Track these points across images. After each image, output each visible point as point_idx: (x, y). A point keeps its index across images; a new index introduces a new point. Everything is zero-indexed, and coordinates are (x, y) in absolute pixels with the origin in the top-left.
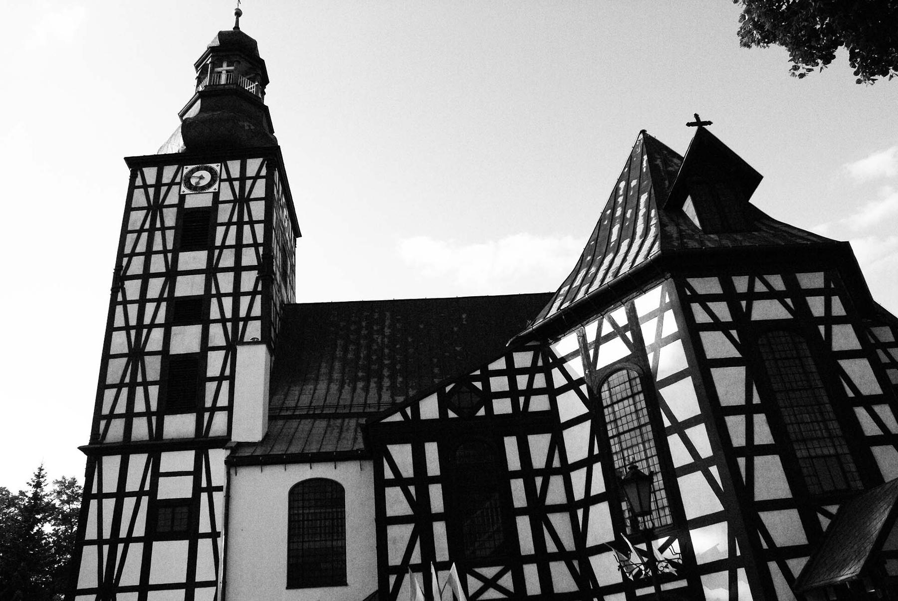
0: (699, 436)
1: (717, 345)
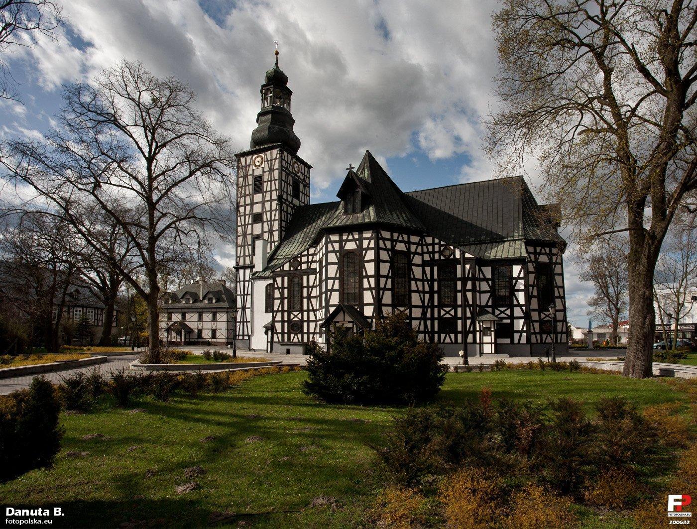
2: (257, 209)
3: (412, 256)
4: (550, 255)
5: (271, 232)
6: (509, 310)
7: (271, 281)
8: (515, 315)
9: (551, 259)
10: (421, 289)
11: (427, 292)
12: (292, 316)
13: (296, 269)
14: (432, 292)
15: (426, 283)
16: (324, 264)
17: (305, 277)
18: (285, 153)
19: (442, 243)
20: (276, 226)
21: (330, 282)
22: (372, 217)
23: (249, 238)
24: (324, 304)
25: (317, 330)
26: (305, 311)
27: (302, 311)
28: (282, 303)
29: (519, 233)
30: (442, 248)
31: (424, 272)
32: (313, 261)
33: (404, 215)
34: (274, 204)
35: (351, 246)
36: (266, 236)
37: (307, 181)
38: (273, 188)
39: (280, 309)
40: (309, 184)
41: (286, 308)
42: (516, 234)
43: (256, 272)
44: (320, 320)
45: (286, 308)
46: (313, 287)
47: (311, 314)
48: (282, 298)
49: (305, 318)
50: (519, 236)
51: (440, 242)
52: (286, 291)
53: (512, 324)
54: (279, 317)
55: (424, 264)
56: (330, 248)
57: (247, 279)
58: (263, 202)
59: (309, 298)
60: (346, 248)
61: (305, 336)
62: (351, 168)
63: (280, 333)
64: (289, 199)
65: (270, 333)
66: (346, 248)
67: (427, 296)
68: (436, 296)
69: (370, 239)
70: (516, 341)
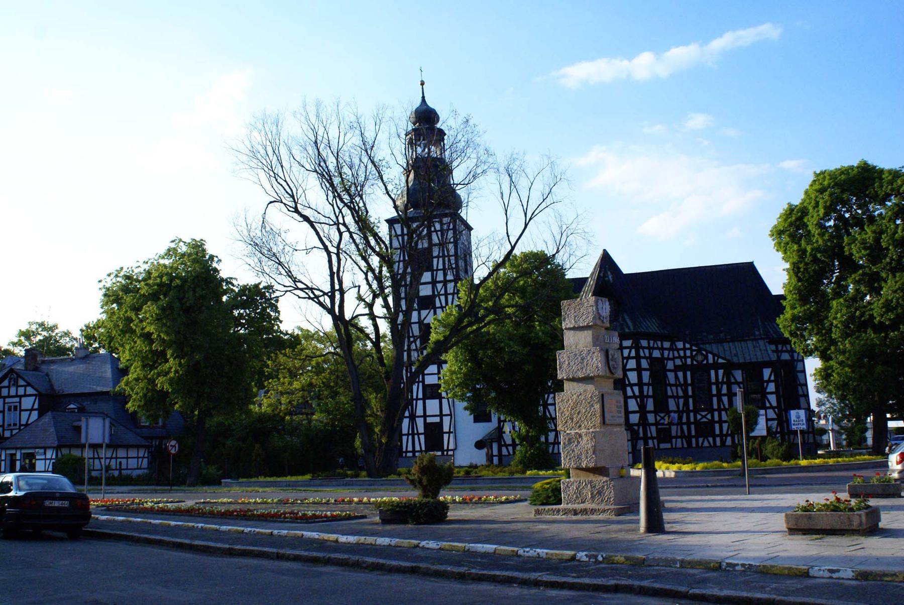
0: (636, 389)
11: (681, 397)
14: (686, 397)
15: (679, 388)
19: (694, 348)
31: (677, 377)
55: (676, 369)
67: (681, 401)
68: (691, 400)
69: (630, 348)
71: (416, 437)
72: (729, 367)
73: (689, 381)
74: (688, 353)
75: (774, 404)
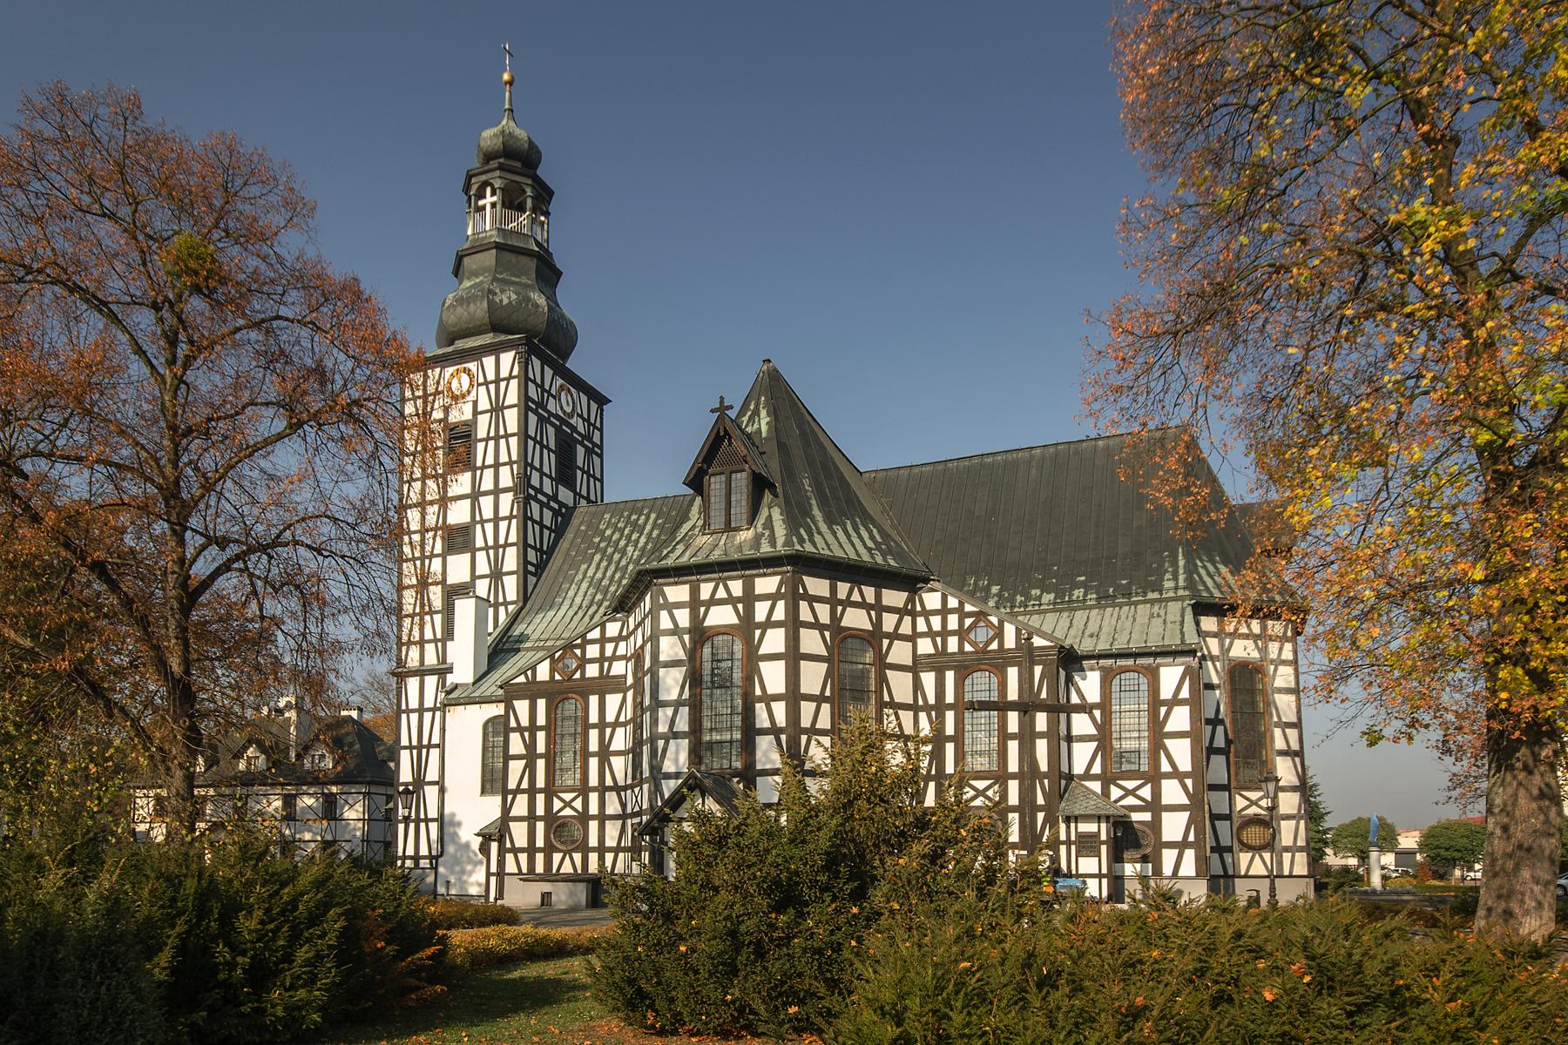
1: (811, 642)
2: (459, 514)
3: (886, 642)
4: (1262, 638)
5: (496, 575)
6: (1148, 787)
7: (498, 710)
8: (1165, 801)
9: (1264, 651)
10: (909, 730)
12: (557, 804)
13: (570, 679)
15: (923, 716)
16: (647, 664)
17: (594, 700)
18: (537, 363)
19: (968, 608)
20: (511, 560)
21: (665, 714)
22: (780, 541)
23: (436, 595)
24: (646, 774)
25: (627, 842)
26: (594, 789)
27: (584, 790)
28: (530, 767)
29: (1175, 578)
30: (968, 622)
31: (917, 686)
32: (614, 658)
33: (865, 535)
34: (506, 500)
35: (721, 616)
36: (482, 588)
37: (596, 439)
38: (504, 458)
39: (525, 785)
40: (601, 447)
41: (541, 782)
42: (1168, 584)
43: (456, 687)
44: (634, 815)
45: (541, 782)
46: (616, 724)
47: (611, 797)
48: (530, 757)
49: (594, 809)
50: (1176, 588)
51: (961, 604)
52: (541, 736)
53: (1156, 825)
54: (520, 807)
55: (916, 666)
56: (665, 622)
57: (429, 703)
58: (475, 496)
59: (605, 754)
60: (706, 624)
61: (593, 858)
62: (722, 408)
63: (522, 850)
64: (548, 487)
65: (494, 846)
66: (706, 624)
68: (950, 748)
69: (773, 598)
70: (1167, 870)
71: (423, 825)
72: (1070, 660)
73: (950, 698)
74: (953, 622)
75: (1185, 765)
